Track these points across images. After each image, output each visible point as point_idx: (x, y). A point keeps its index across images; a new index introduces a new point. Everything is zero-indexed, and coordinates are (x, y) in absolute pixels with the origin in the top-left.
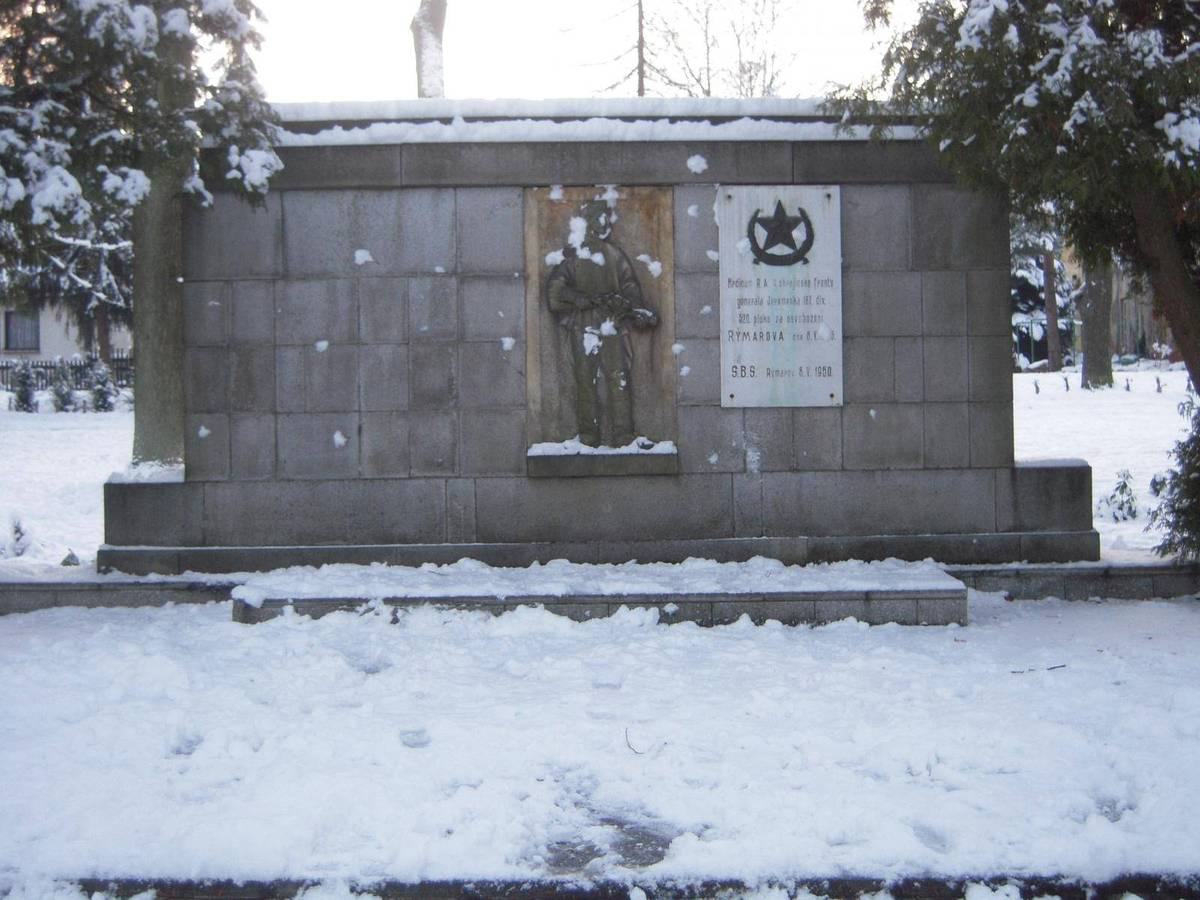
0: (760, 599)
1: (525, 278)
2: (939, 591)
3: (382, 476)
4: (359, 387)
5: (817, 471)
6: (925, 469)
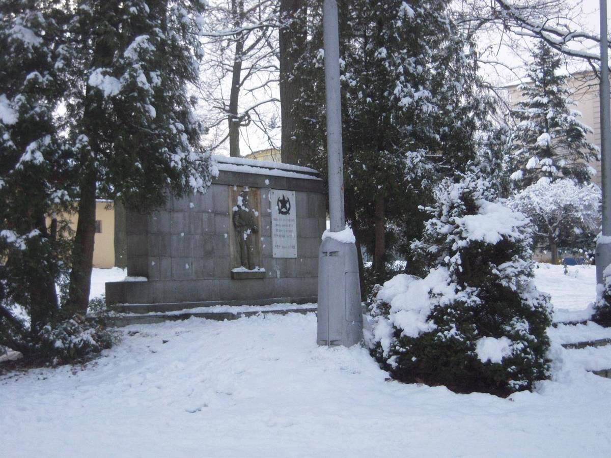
1: (229, 215)
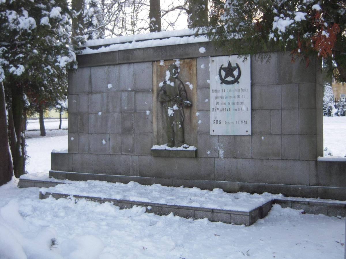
0: (177, 207)
1: (153, 91)
2: (238, 212)
3: (114, 154)
4: (109, 126)
5: (243, 158)
6: (282, 159)
